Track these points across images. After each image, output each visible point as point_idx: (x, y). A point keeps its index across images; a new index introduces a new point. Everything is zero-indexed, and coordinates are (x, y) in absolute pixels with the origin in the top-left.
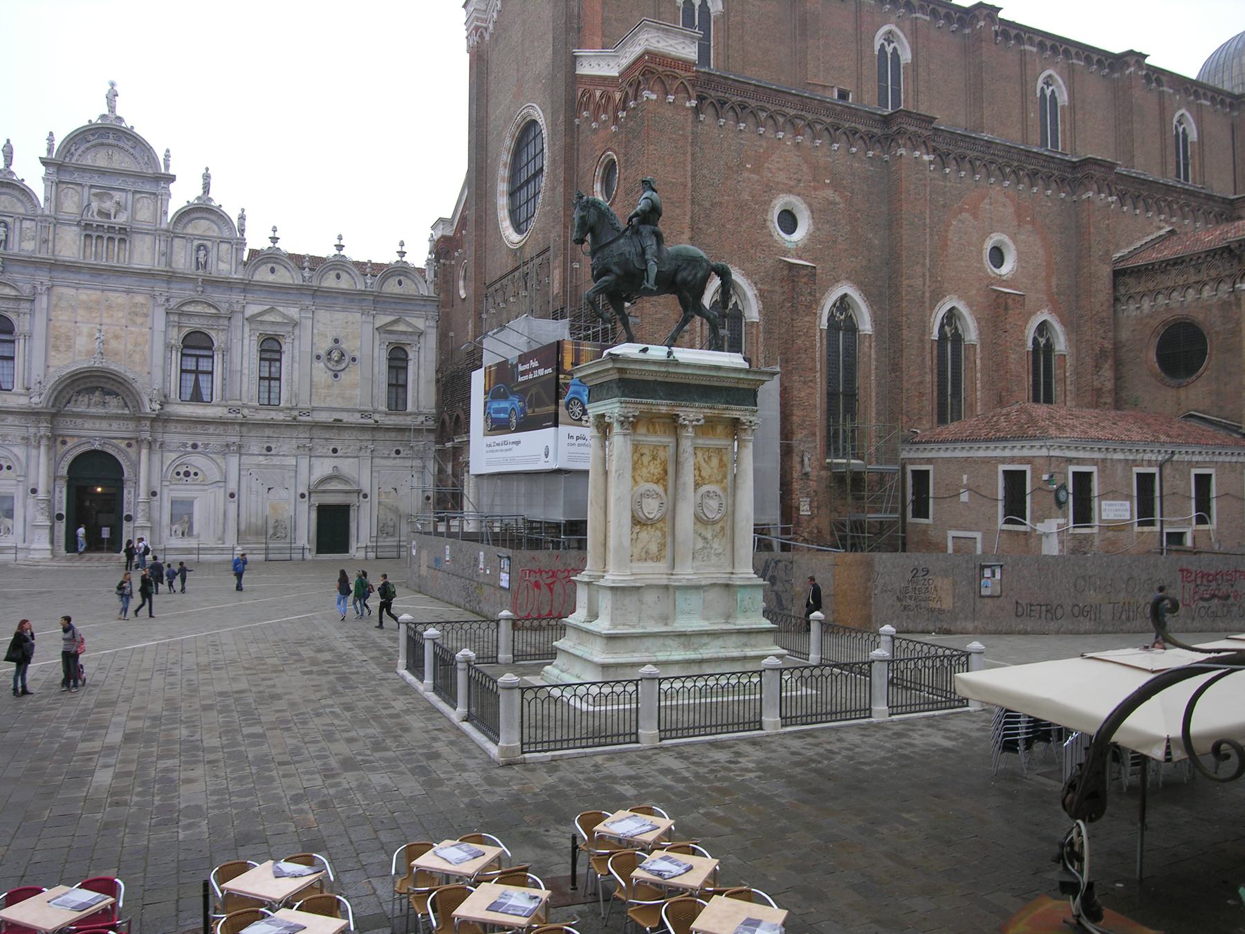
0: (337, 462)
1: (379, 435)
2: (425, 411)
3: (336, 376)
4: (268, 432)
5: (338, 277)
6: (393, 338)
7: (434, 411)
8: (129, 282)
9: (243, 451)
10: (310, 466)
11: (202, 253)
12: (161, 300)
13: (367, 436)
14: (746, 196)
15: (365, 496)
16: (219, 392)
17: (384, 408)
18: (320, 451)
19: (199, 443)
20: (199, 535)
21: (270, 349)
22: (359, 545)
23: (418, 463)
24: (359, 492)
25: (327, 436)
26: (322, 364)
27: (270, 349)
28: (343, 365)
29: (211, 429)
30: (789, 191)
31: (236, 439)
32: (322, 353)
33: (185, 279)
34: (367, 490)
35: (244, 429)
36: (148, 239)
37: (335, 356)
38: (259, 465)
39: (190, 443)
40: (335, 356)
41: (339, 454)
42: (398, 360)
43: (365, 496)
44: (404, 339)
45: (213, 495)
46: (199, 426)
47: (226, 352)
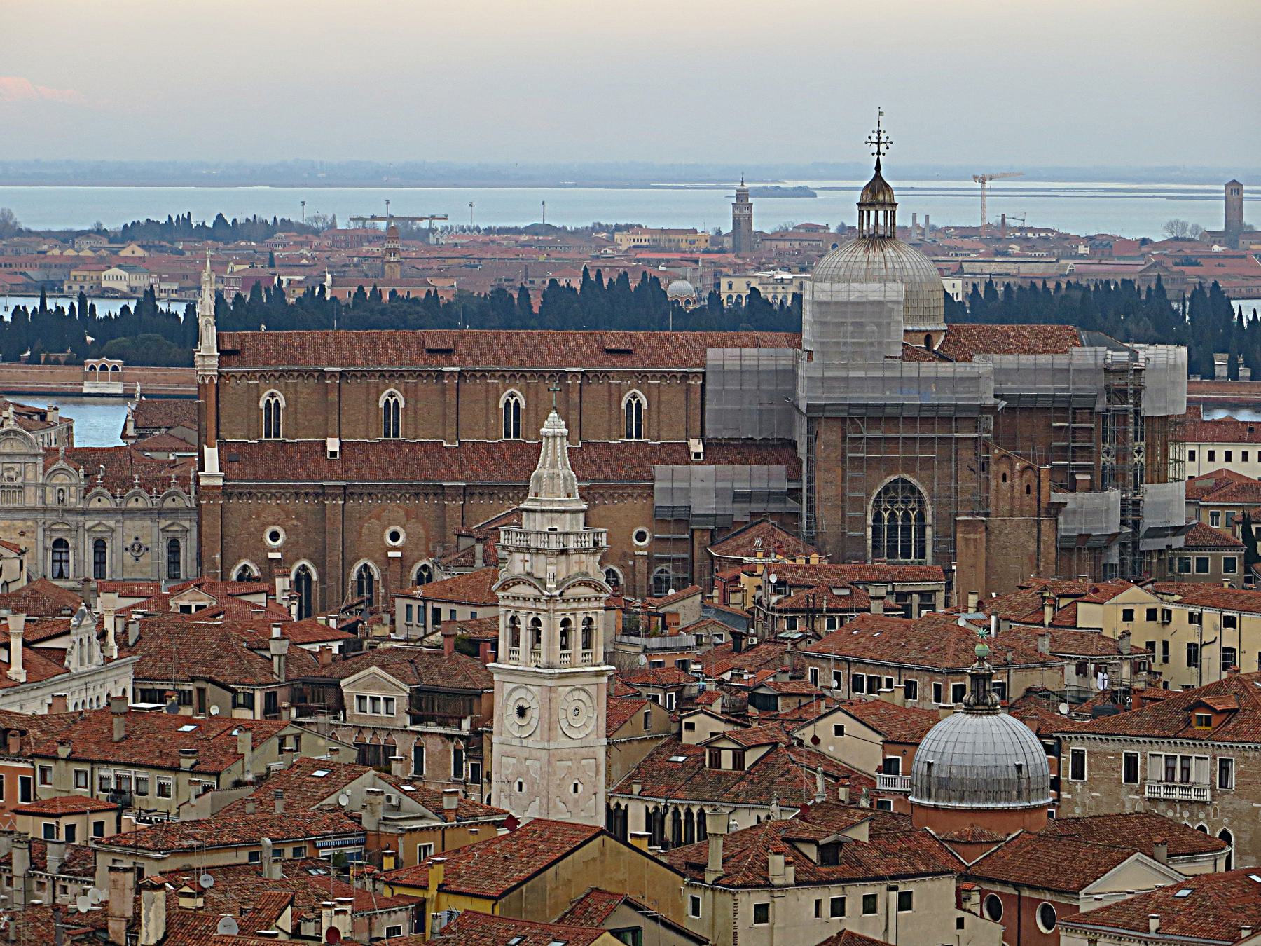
5: (137, 500)
6: (170, 535)
8: (23, 515)
11: (61, 494)
12: (40, 523)
14: (253, 530)
21: (100, 546)
27: (100, 546)
30: (274, 524)
32: (129, 546)
33: (52, 510)
36: (33, 488)
37: (136, 548)
40: (136, 548)
42: (174, 547)
44: (177, 535)
47: (76, 549)
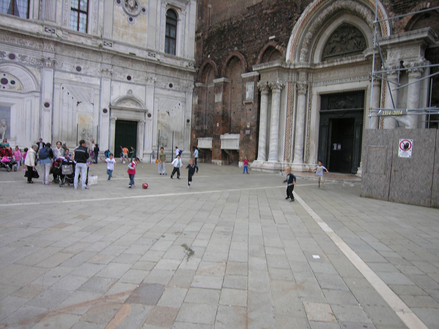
0: (131, 87)
1: (160, 71)
2: (189, 58)
3: (131, 19)
4: (78, 54)
7: (194, 60)
9: (57, 67)
10: (111, 88)
13: (151, 70)
15: (149, 115)
16: (36, 11)
17: (163, 51)
18: (118, 76)
19: (17, 55)
20: (16, 138)
22: (145, 152)
23: (182, 95)
24: (145, 112)
25: (124, 66)
26: (121, 8)
28: (136, 13)
29: (28, 43)
31: (52, 56)
34: (151, 111)
35: (58, 49)
38: (70, 82)
39: (8, 53)
41: (132, 80)
43: (149, 115)
45: (29, 103)
46: (16, 39)
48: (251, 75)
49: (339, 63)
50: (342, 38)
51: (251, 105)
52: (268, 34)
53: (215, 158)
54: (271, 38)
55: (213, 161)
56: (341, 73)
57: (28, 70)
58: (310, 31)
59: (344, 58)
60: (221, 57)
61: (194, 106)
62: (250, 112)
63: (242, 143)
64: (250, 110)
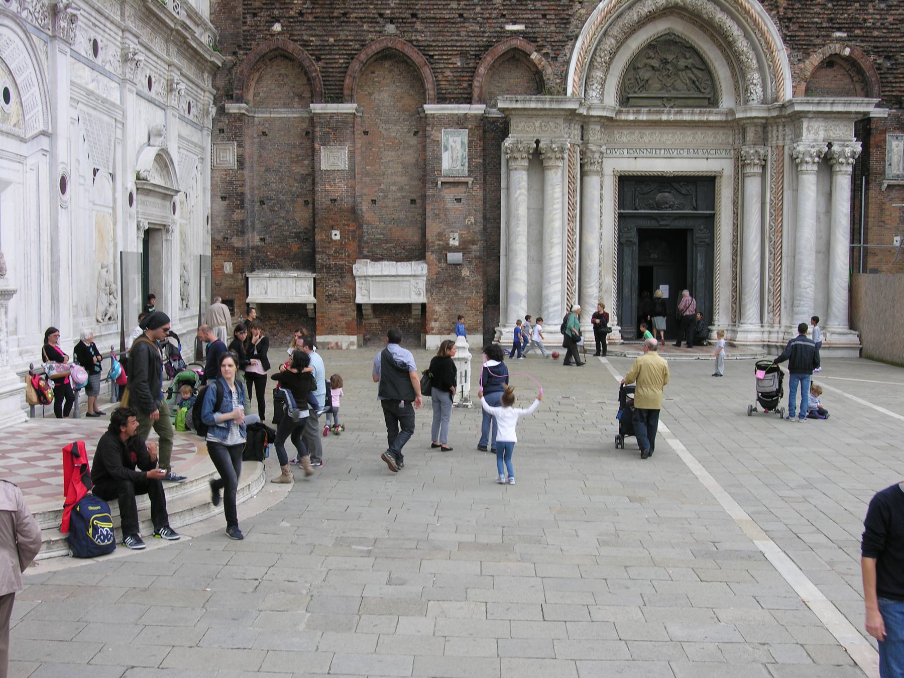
48: (456, 112)
49: (672, 117)
50: (665, 62)
51: (462, 189)
52: (503, 16)
53: (332, 331)
54: (510, 27)
55: (319, 339)
56: (668, 137)
57: (33, 47)
58: (615, 37)
59: (685, 110)
60: (332, 40)
61: (217, 174)
62: (457, 205)
63: (433, 285)
64: (459, 200)
